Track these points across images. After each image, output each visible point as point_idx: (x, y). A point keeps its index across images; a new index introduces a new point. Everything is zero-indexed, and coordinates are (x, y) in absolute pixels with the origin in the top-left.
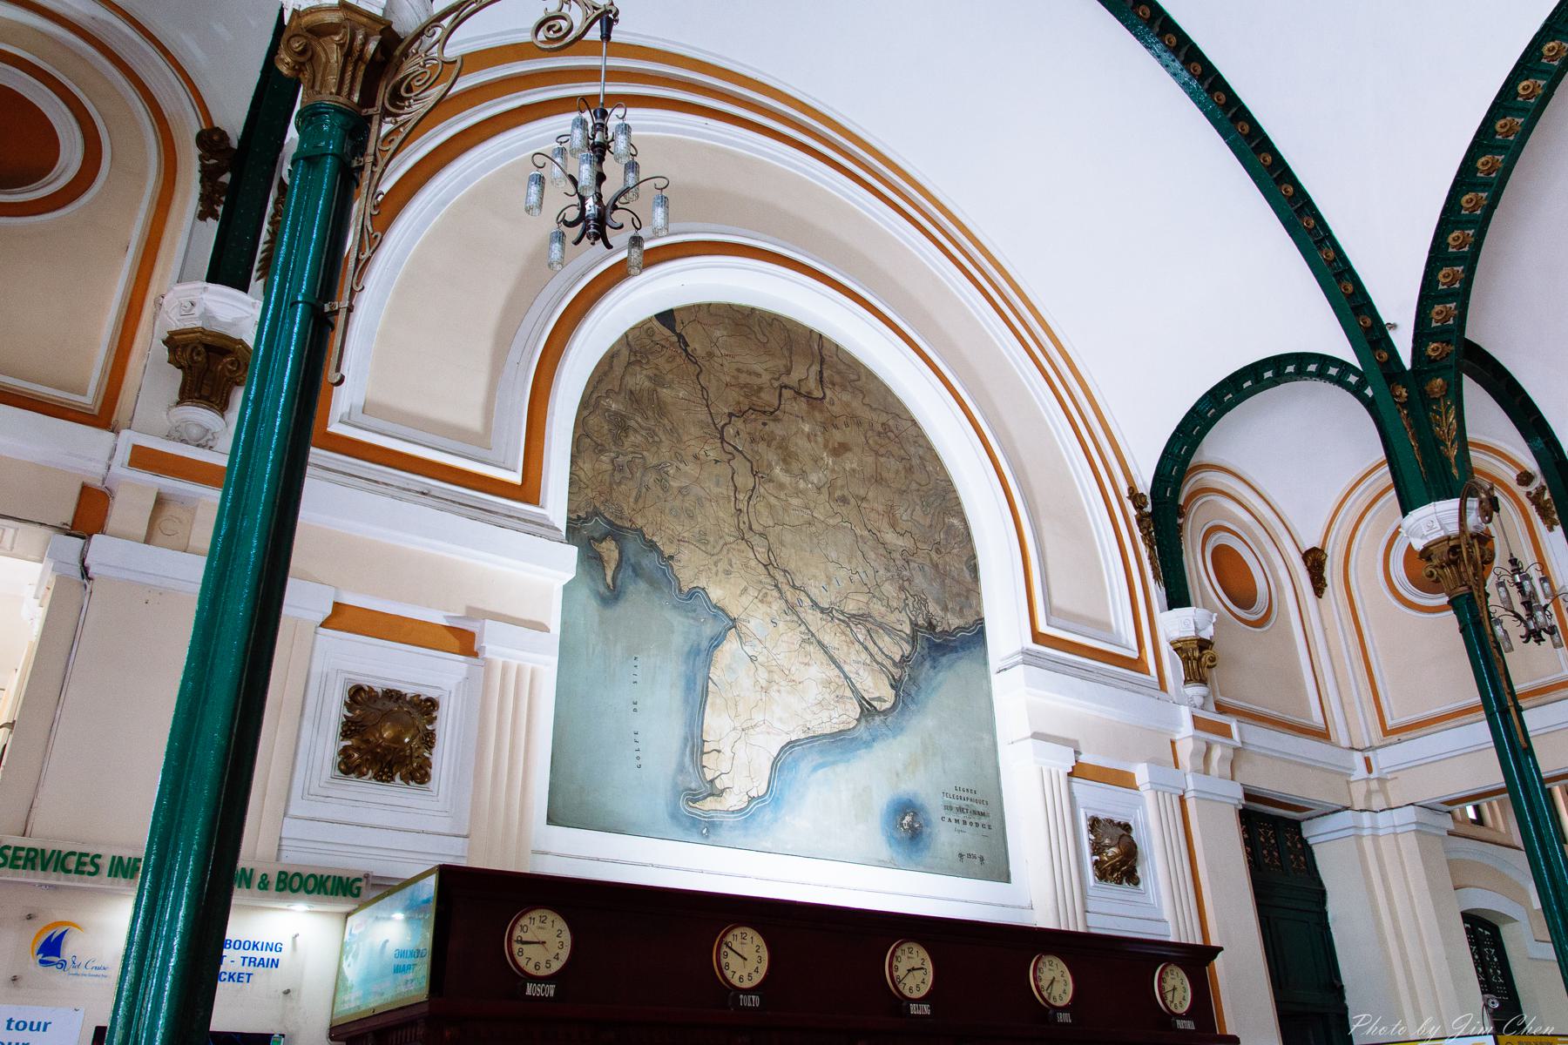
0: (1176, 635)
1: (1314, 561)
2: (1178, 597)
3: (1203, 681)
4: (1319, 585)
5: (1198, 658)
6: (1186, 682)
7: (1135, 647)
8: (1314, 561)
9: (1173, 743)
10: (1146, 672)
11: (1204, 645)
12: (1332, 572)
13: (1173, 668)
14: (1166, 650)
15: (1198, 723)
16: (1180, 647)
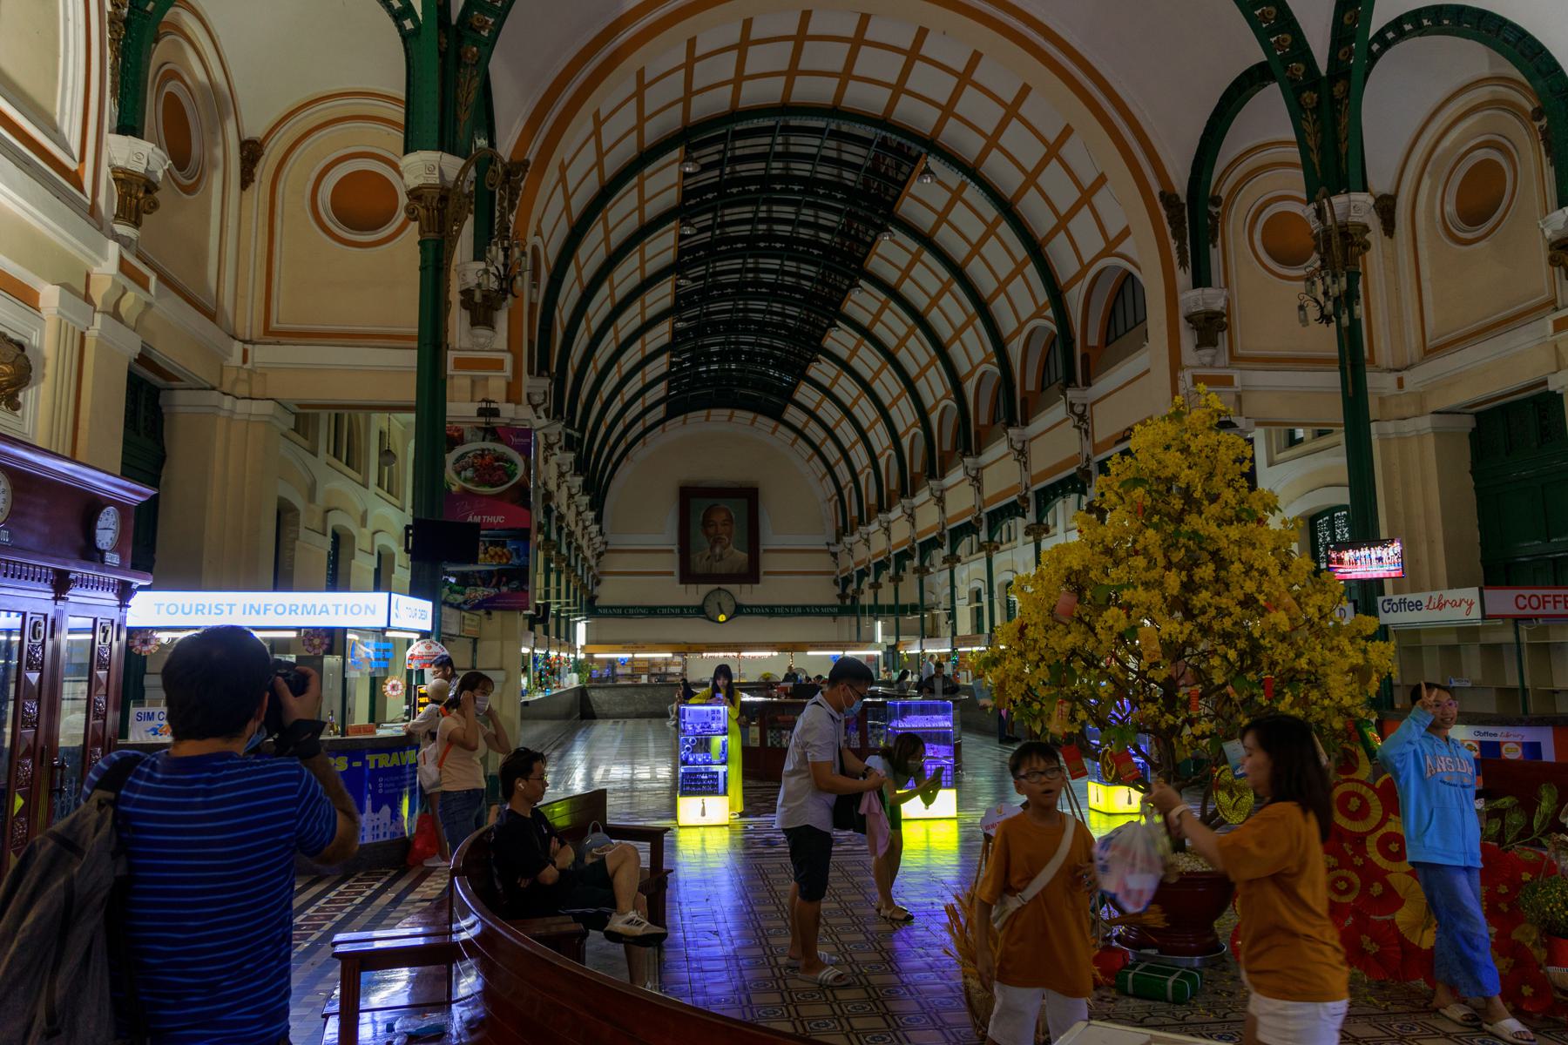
0: (120, 163)
1: (251, 152)
2: (129, 126)
3: (137, 224)
4: (247, 179)
5: (136, 196)
6: (117, 216)
7: (77, 157)
8: (251, 152)
9: (88, 276)
10: (81, 190)
11: (150, 186)
12: (264, 170)
13: (107, 200)
14: (105, 172)
15: (123, 266)
16: (124, 179)
